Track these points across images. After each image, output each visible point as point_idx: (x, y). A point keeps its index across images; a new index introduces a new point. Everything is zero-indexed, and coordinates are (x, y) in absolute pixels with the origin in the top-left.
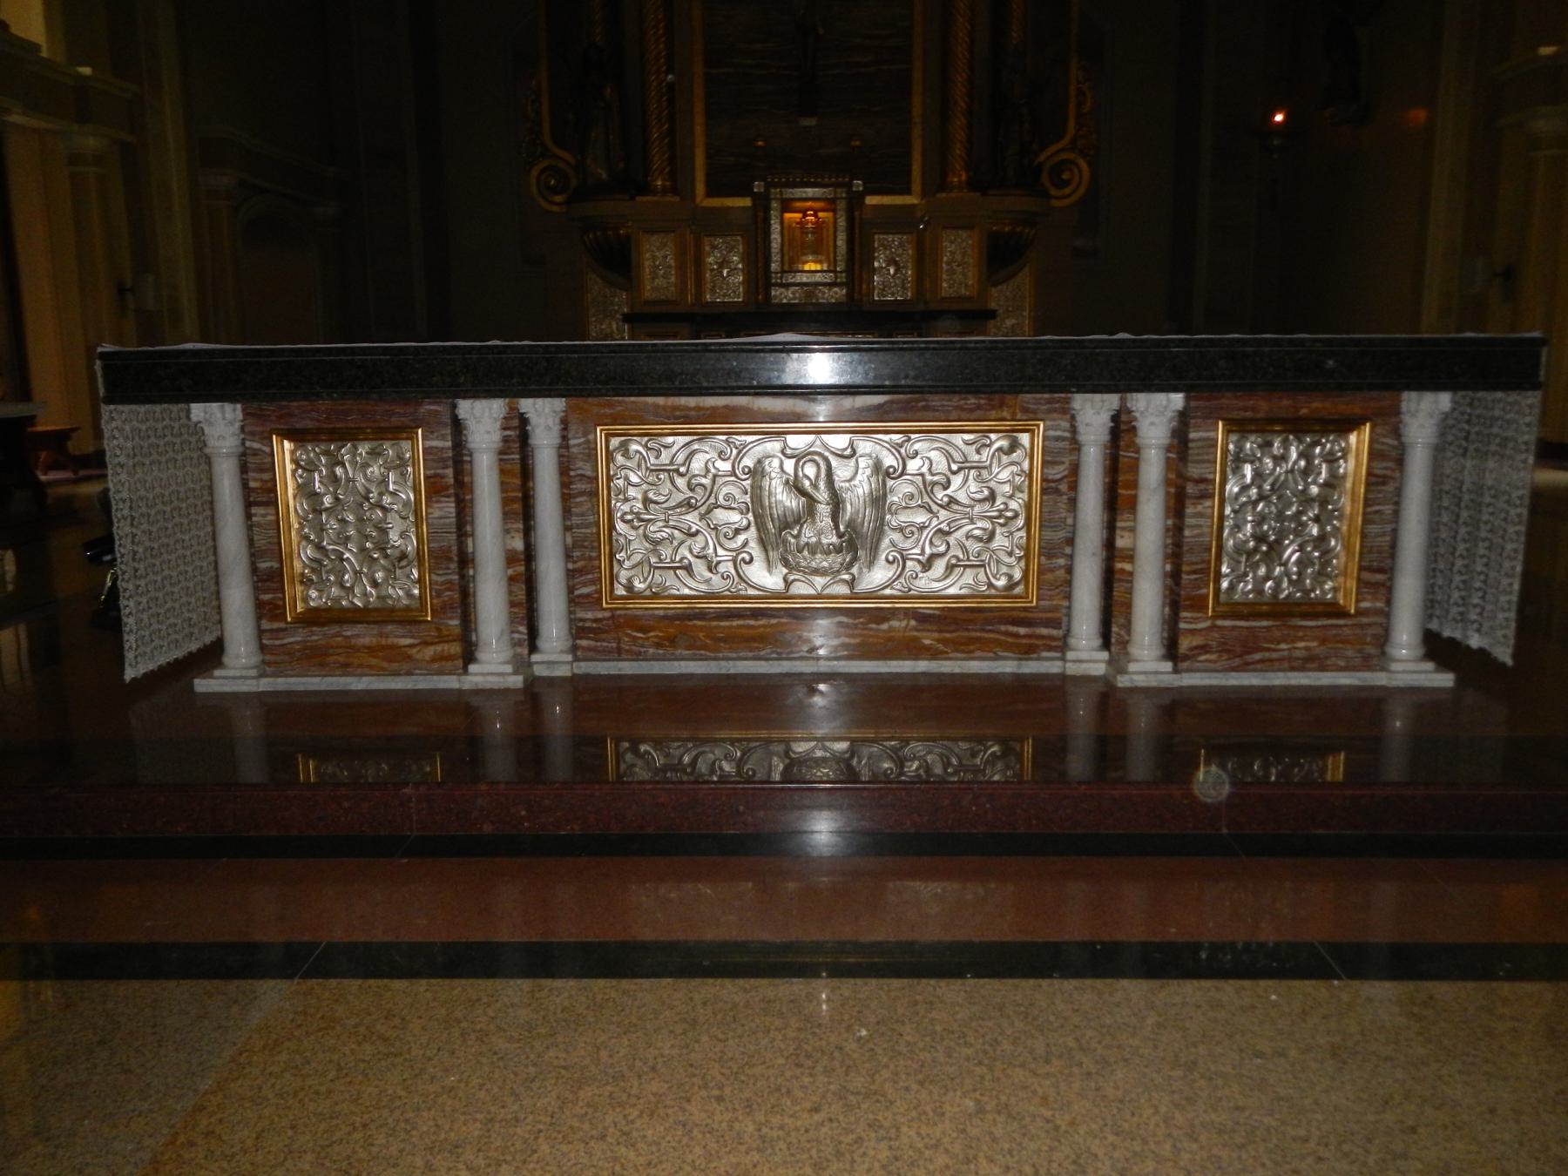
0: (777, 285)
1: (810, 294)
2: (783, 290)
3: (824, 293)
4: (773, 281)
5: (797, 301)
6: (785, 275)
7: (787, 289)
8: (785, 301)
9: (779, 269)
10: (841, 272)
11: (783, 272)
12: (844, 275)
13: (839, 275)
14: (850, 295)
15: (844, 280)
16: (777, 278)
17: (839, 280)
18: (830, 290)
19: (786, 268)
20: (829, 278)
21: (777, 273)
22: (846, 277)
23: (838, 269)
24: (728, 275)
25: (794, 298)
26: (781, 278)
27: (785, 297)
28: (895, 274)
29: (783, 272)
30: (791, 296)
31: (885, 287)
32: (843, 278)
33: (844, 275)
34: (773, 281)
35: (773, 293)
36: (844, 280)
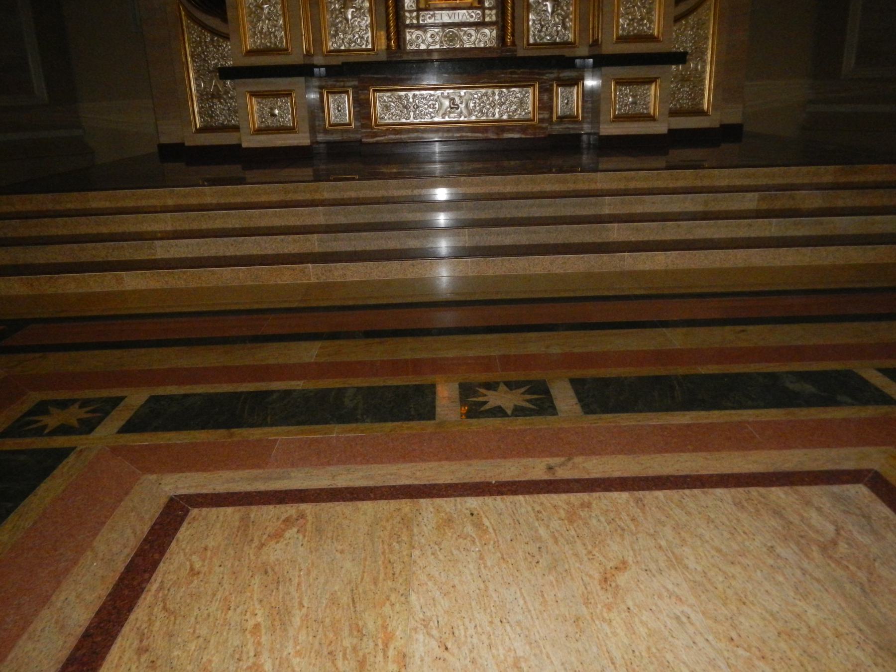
0: (411, 26)
1: (452, 38)
2: (419, 32)
3: (470, 35)
4: (408, 22)
5: (438, 47)
6: (422, 13)
7: (425, 32)
8: (423, 47)
9: (415, 8)
10: (490, 9)
11: (419, 10)
12: (494, 12)
13: (487, 12)
14: (502, 38)
15: (494, 18)
16: (411, 18)
17: (487, 19)
18: (477, 32)
19: (422, 6)
20: (473, 16)
21: (411, 12)
22: (497, 15)
23: (487, 5)
24: (353, 17)
25: (434, 42)
26: (418, 18)
27: (423, 42)
28: (553, 12)
29: (419, 10)
30: (430, 40)
31: (542, 26)
32: (491, 16)
33: (494, 12)
34: (408, 22)
35: (408, 37)
36: (494, 18)
